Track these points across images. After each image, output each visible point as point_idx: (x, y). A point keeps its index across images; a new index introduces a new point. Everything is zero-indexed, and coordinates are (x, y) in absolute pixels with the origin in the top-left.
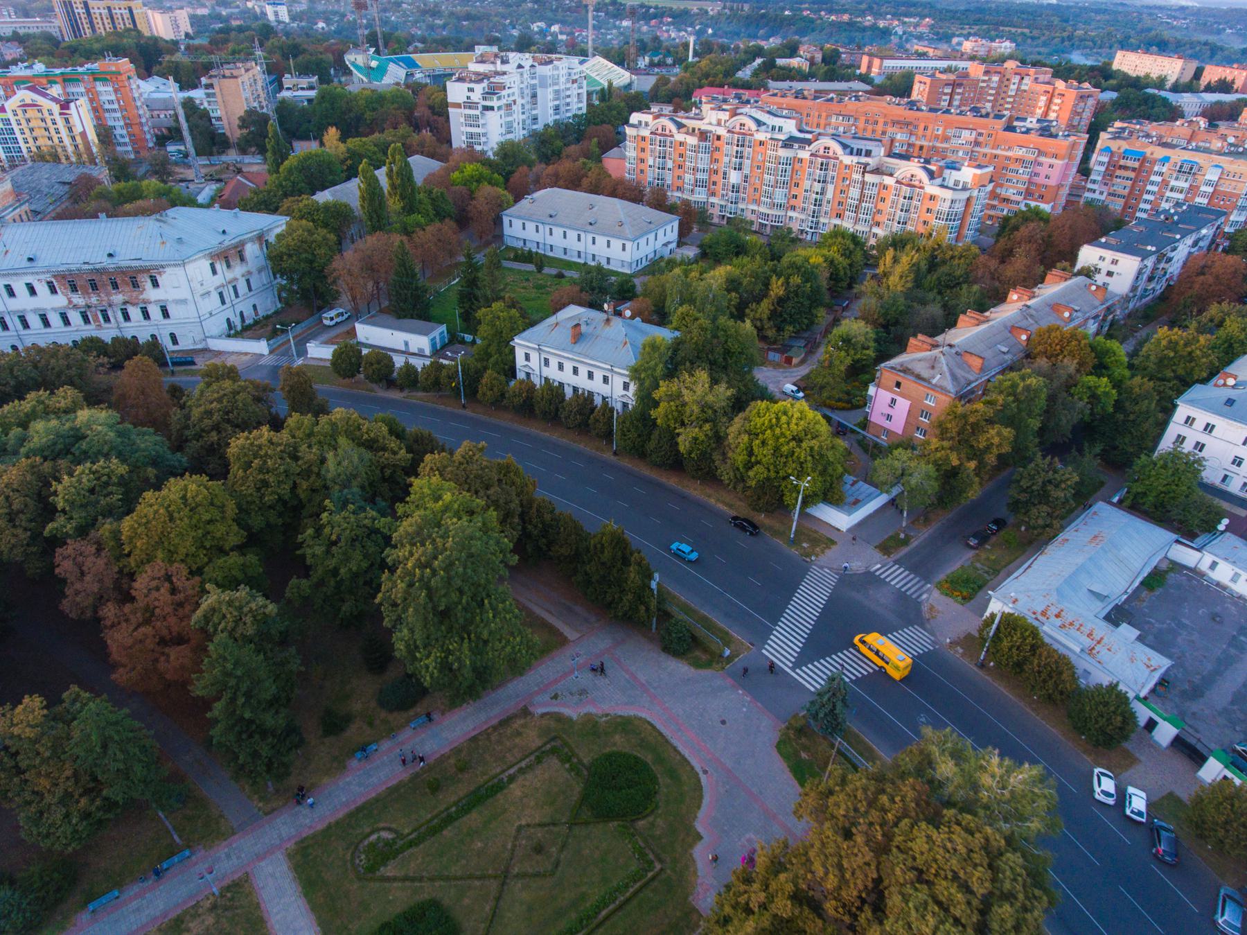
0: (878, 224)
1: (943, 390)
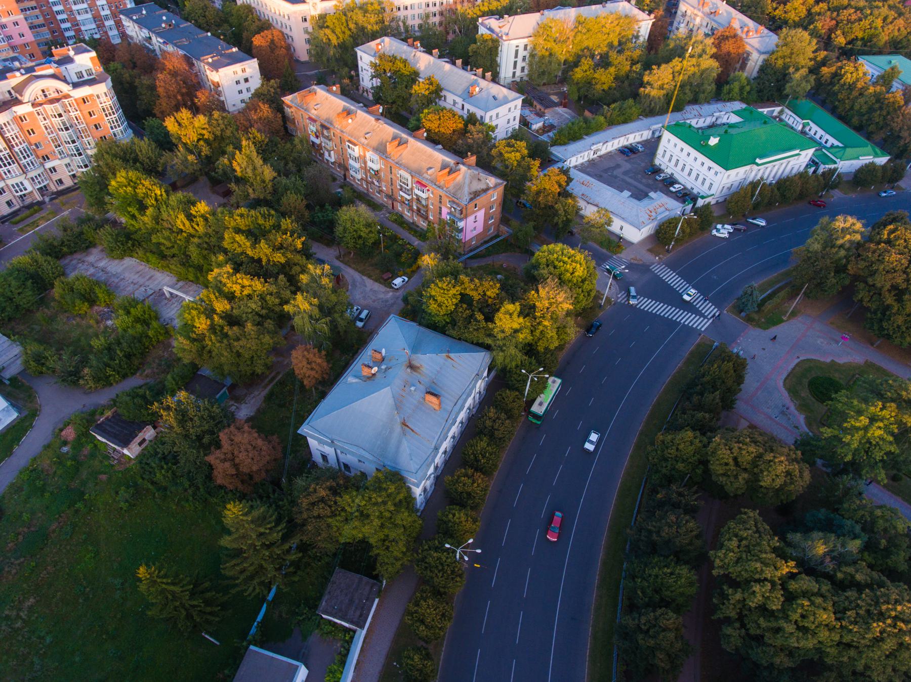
0: (46, 158)
1: (499, 184)
